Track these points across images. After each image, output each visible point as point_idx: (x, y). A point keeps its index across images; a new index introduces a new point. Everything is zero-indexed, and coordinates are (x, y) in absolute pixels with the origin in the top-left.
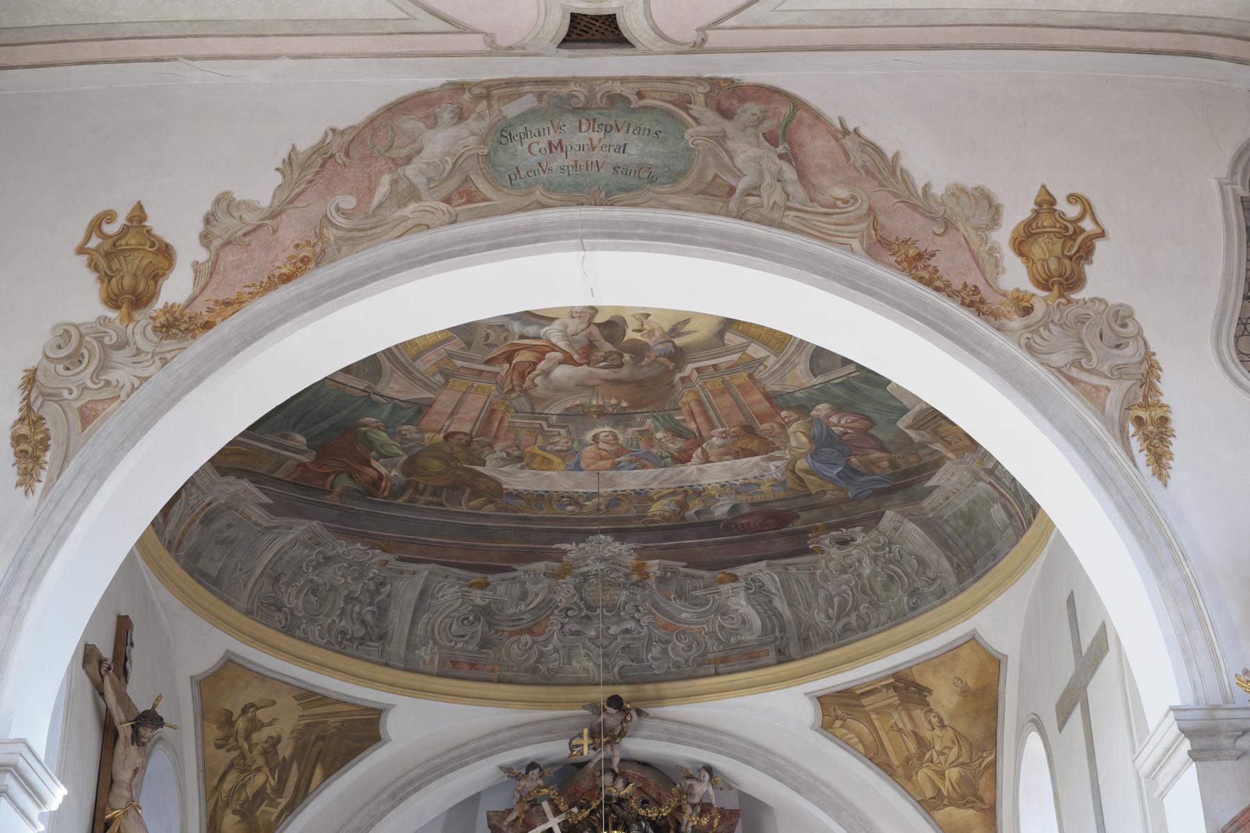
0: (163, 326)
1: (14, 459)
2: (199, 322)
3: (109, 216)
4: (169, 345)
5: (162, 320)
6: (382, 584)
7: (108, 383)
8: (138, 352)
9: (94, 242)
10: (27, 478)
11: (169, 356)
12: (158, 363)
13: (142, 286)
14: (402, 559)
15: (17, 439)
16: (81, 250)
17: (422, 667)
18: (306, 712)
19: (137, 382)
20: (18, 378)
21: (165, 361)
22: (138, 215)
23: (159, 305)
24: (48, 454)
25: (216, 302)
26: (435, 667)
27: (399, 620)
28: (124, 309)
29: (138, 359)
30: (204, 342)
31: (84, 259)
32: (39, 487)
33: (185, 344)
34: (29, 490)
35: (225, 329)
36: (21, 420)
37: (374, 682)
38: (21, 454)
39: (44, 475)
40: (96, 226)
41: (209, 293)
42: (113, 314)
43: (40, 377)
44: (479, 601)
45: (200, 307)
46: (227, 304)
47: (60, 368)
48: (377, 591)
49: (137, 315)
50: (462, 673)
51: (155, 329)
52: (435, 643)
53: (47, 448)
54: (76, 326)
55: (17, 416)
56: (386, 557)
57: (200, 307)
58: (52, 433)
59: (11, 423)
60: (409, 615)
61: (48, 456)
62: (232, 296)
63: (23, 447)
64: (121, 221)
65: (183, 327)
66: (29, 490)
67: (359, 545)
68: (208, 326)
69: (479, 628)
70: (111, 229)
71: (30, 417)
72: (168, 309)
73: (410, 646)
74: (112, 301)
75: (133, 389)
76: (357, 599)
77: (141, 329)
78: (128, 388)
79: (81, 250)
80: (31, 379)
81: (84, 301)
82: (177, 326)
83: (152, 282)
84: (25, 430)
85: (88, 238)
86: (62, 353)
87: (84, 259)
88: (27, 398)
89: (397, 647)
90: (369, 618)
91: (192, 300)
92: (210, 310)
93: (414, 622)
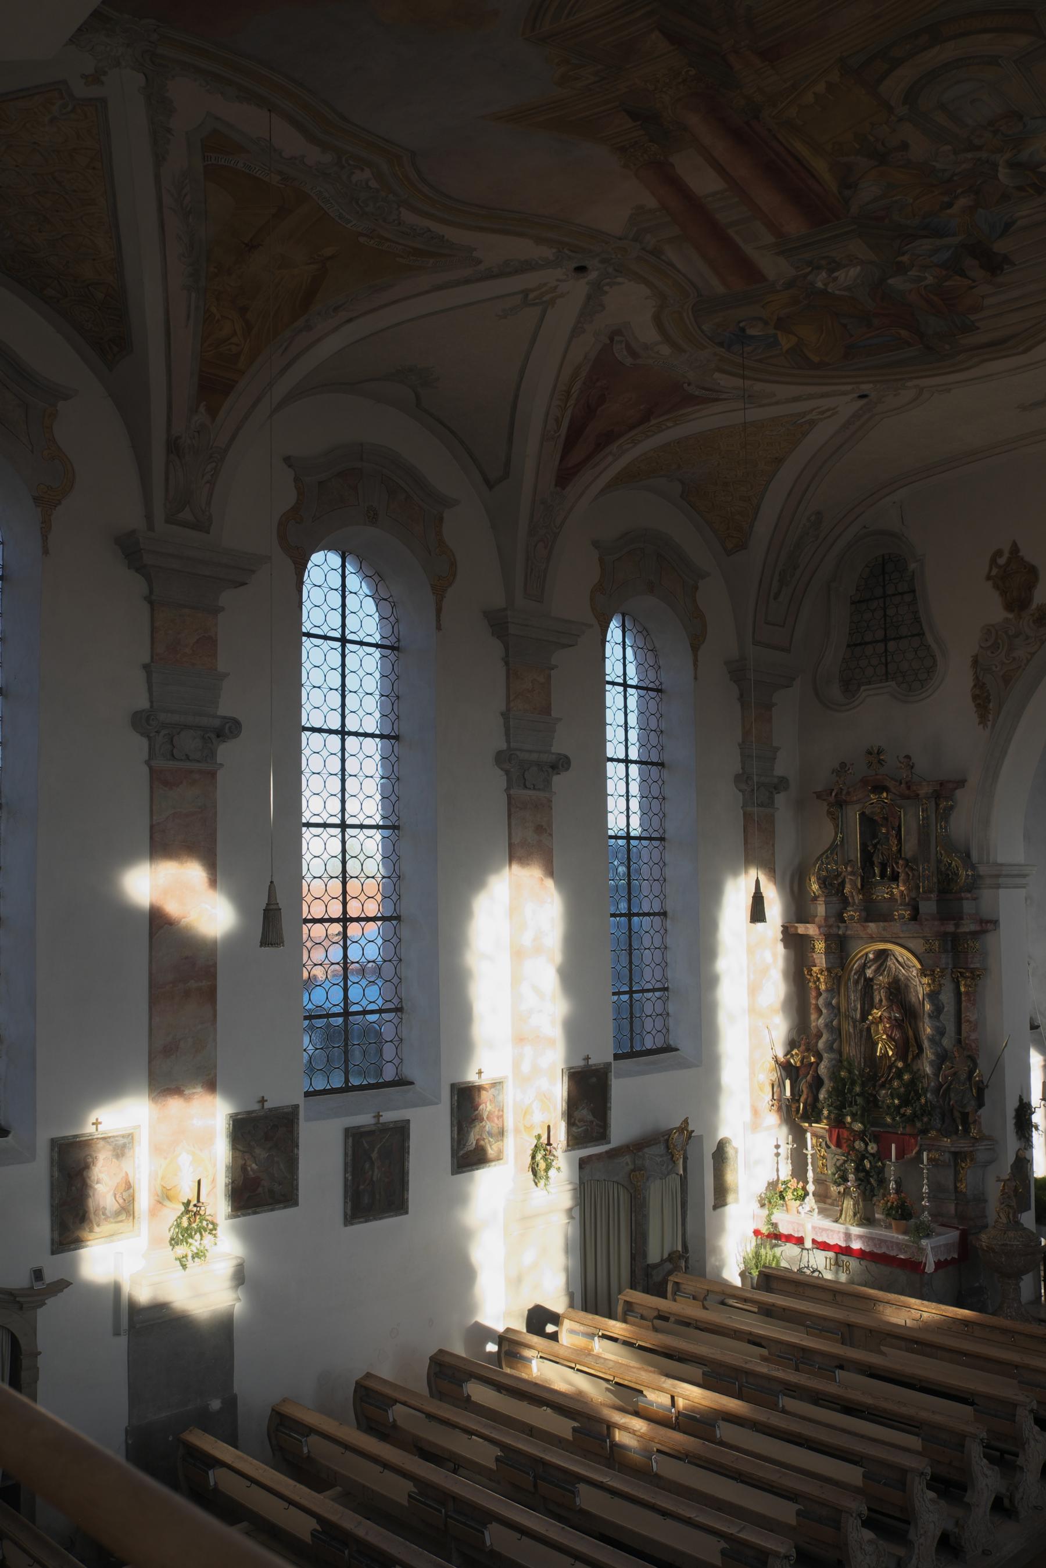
3: (999, 553)
7: (1014, 659)
9: (994, 572)
10: (983, 719)
15: (975, 697)
16: (989, 578)
22: (1015, 549)
31: (990, 583)
32: (989, 724)
36: (975, 686)
38: (978, 706)
39: (991, 717)
40: (993, 561)
42: (1011, 616)
53: (989, 702)
55: (972, 684)
61: (991, 705)
64: (1006, 555)
70: (1002, 561)
74: (1009, 607)
79: (989, 578)
80: (975, 662)
81: (995, 612)
84: (978, 692)
85: (990, 570)
87: (990, 583)
88: (976, 673)
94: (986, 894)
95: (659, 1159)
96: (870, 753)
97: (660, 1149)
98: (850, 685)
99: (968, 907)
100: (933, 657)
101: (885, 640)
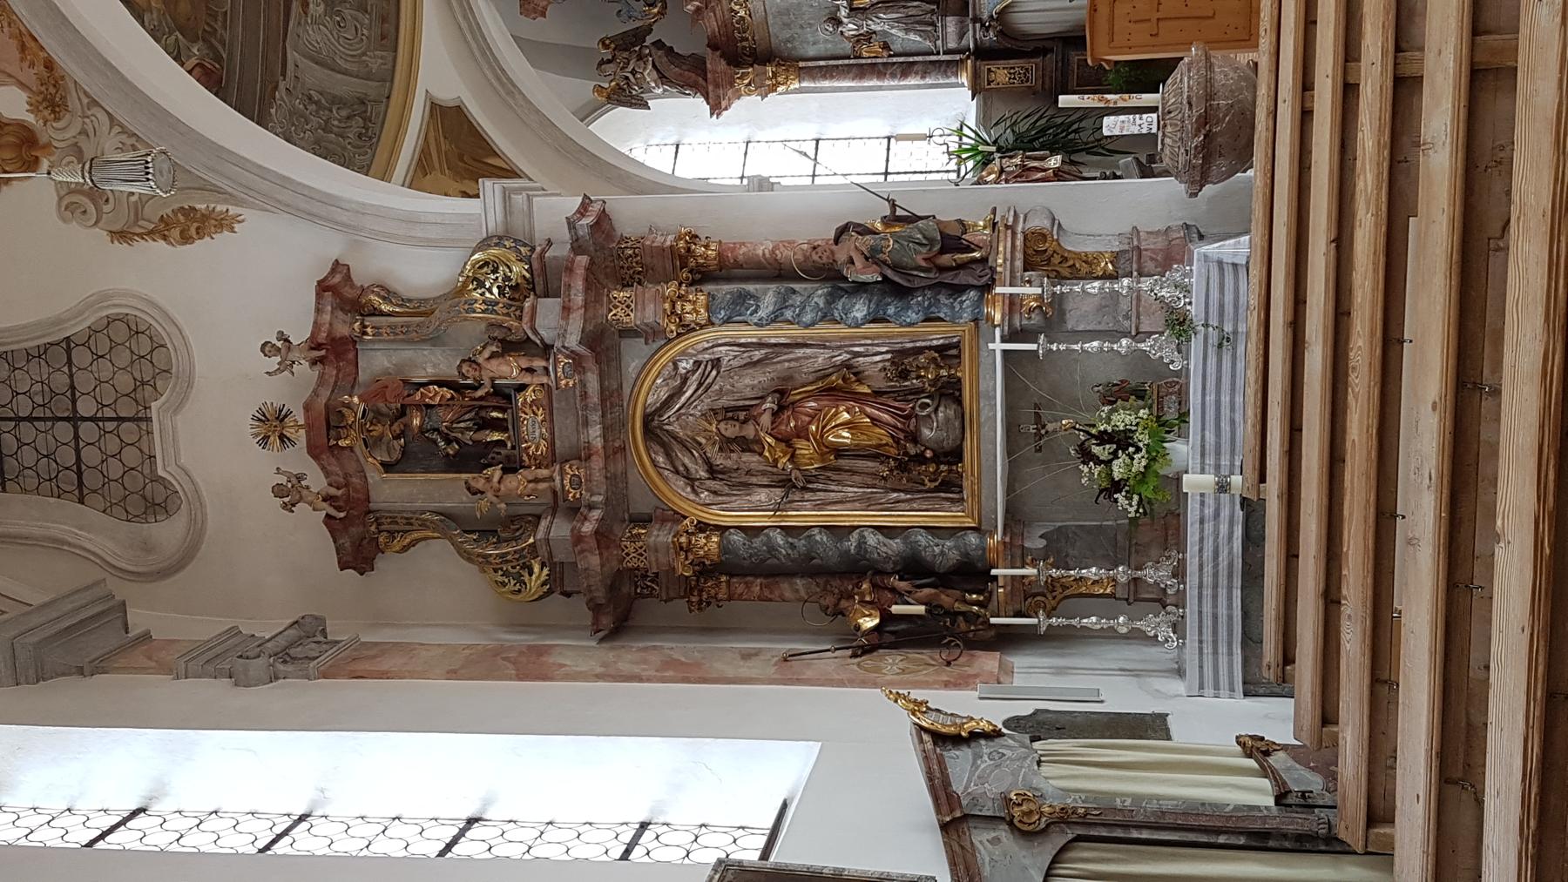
0: (53, 111)
1: (207, 239)
2: (46, 75)
4: (73, 102)
5: (46, 113)
6: (310, 98)
8: (84, 132)
10: (224, 223)
11: (85, 101)
12: (95, 110)
13: (12, 139)
14: (284, 74)
15: (186, 239)
17: (389, 66)
18: (437, 165)
19: (117, 129)
20: (121, 248)
21: (94, 103)
23: (30, 118)
24: (198, 206)
25: (22, 60)
26: (388, 55)
27: (345, 86)
28: (37, 154)
29: (91, 134)
30: (67, 63)
32: (233, 210)
33: (71, 86)
34: (237, 219)
35: (53, 46)
36: (165, 238)
37: (406, 107)
38: (200, 233)
39: (220, 208)
41: (13, 69)
42: (45, 164)
43: (117, 228)
44: (321, 8)
45: (30, 76)
46: (23, 48)
47: (106, 208)
48: (317, 103)
49: (43, 139)
50: (393, 30)
51: (57, 119)
52: (364, 54)
53: (193, 209)
54: (61, 199)
55: (162, 242)
56: (282, 85)
57: (30, 76)
58: (176, 206)
59: (169, 247)
60: (339, 76)
62: (14, 43)
63: (193, 231)
65: (52, 90)
66: (237, 219)
67: (273, 111)
68: (49, 65)
69: (347, 13)
71: (162, 230)
72: (34, 108)
73: (368, 77)
75: (124, 130)
76: (326, 122)
77: (58, 134)
78: (123, 137)
80: (122, 236)
82: (52, 94)
83: (7, 129)
84: (176, 233)
86: (91, 208)
88: (141, 236)
89: (371, 89)
90: (344, 113)
91: (22, 85)
92: (32, 65)
93: (345, 73)
94: (541, 232)
95: (985, 763)
96: (266, 438)
97: (959, 762)
98: (154, 501)
99: (561, 251)
100: (111, 321)
101: (75, 419)
